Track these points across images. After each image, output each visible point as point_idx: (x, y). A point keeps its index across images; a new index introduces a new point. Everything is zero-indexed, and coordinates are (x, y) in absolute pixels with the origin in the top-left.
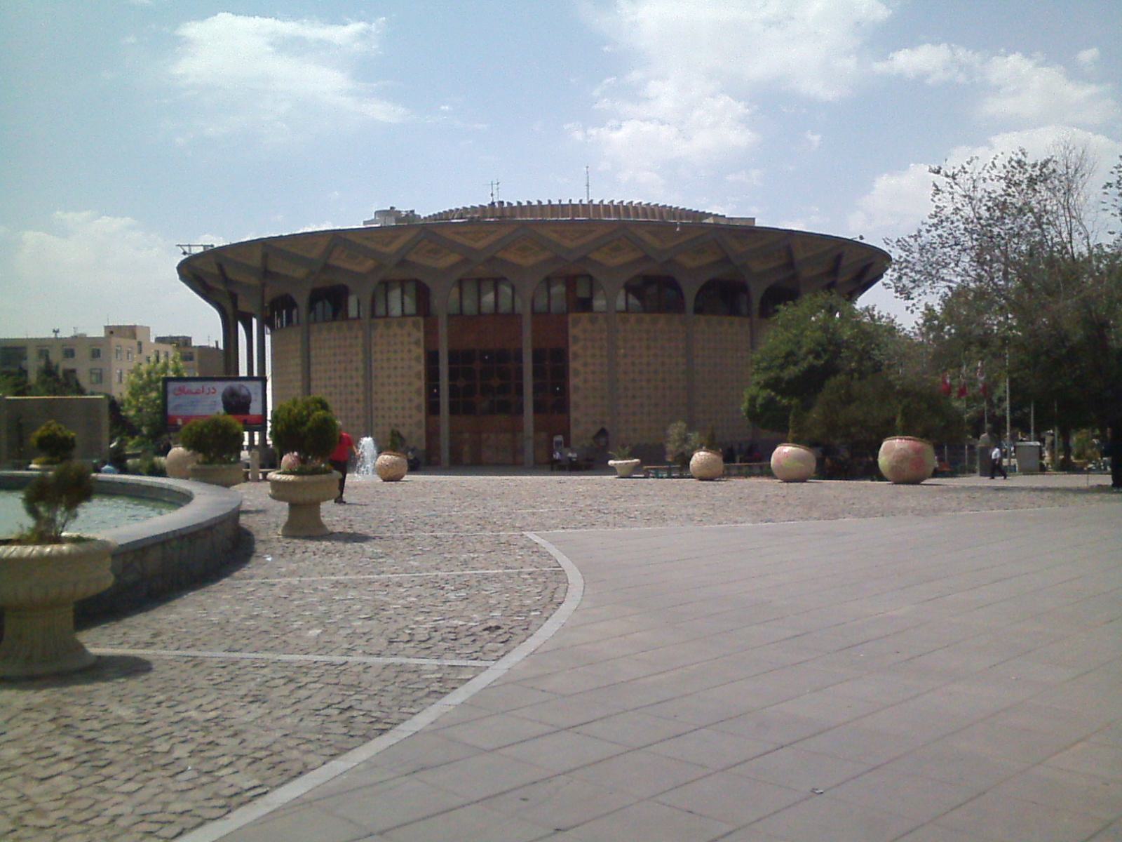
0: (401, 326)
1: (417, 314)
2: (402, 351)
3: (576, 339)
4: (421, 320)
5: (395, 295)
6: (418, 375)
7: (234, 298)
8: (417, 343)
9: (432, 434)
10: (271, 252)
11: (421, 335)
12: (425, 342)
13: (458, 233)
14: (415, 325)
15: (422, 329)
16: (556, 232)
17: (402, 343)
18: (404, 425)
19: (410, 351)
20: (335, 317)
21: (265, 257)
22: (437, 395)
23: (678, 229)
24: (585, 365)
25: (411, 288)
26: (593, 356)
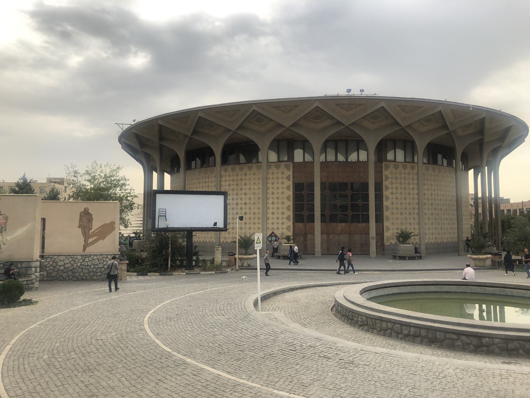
0: (278, 167)
4: (291, 164)
8: (288, 178)
11: (290, 173)
14: (287, 167)
15: (291, 169)
17: (278, 178)
18: (278, 228)
24: (392, 193)
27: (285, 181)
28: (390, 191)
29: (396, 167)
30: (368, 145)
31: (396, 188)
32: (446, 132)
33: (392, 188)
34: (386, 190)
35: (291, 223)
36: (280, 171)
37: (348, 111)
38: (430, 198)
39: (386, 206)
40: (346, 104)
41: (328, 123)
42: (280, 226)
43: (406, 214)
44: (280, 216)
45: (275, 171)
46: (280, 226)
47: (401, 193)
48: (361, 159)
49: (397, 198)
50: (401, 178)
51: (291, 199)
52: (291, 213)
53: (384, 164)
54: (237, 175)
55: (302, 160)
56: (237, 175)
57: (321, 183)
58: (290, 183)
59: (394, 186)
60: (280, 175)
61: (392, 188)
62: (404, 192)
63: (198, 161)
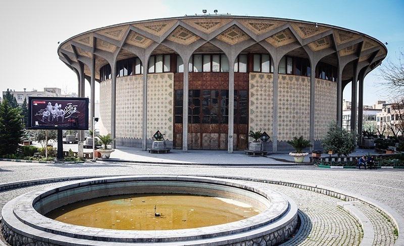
0: (162, 77)
1: (170, 72)
2: (162, 90)
3: (253, 86)
4: (173, 74)
5: (159, 64)
6: (170, 103)
7: (82, 65)
8: (170, 86)
9: (177, 132)
10: (97, 37)
11: (172, 82)
12: (174, 85)
13: (198, 24)
14: (169, 77)
15: (173, 79)
16: (250, 24)
19: (166, 90)
20: (129, 74)
21: (95, 39)
22: (182, 112)
23: (317, 27)
24: (257, 99)
25: (168, 58)
26: (261, 95)
27: (168, 88)
28: (255, 97)
29: (262, 77)
30: (229, 58)
31: (261, 95)
32: (299, 47)
33: (257, 95)
34: (252, 96)
35: (172, 124)
36: (164, 80)
37: (259, 30)
38: (293, 103)
39: (251, 110)
40: (205, 23)
41: (193, 39)
42: (164, 126)
43: (269, 116)
44: (164, 118)
45: (160, 80)
46: (164, 126)
47: (265, 99)
48: (214, 70)
49: (261, 104)
50: (265, 86)
51: (173, 104)
52: (172, 116)
53: (251, 74)
54: (133, 84)
55: (218, 71)
56: (133, 84)
57: (234, 90)
58: (172, 90)
59: (259, 93)
60: (164, 84)
61: (257, 95)
62: (268, 98)
63: (126, 71)
